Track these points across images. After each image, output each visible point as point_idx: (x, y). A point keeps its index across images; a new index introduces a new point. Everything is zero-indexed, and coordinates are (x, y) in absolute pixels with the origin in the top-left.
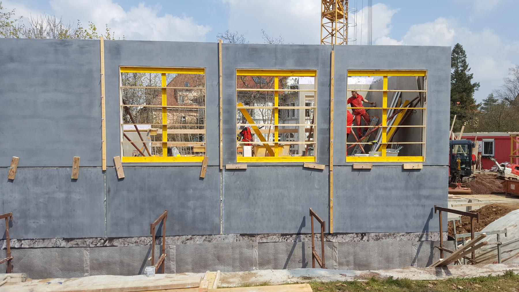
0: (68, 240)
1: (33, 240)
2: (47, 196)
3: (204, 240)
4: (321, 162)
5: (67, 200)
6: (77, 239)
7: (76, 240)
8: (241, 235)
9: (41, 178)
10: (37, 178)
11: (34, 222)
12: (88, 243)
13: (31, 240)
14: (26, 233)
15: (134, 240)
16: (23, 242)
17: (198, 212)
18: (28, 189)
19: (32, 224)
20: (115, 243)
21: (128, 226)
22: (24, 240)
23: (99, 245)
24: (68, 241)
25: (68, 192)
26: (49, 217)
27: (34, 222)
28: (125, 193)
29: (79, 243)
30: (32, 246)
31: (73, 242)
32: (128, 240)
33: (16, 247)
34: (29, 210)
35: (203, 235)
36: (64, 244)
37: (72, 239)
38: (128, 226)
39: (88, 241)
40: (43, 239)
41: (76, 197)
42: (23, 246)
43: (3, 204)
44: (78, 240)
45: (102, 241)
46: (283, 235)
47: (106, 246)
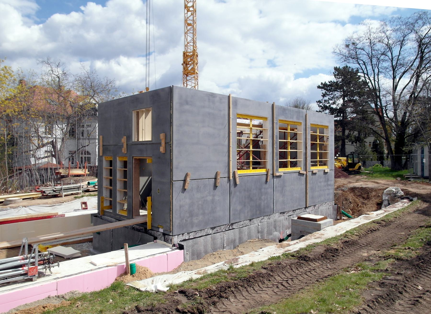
0: (213, 228)
1: (196, 231)
2: (203, 199)
3: (268, 219)
4: (303, 171)
5: (213, 201)
6: (217, 227)
7: (217, 228)
8: (281, 213)
9: (201, 187)
10: (199, 187)
11: (196, 219)
12: (222, 229)
13: (195, 232)
14: (192, 227)
15: (242, 223)
16: (190, 234)
17: (266, 202)
18: (193, 195)
19: (195, 221)
20: (234, 226)
21: (239, 214)
22: (191, 232)
23: (227, 229)
24: (213, 229)
25: (214, 196)
26: (204, 214)
27: (196, 219)
28: (238, 193)
29: (218, 230)
30: (195, 236)
31: (215, 230)
32: (239, 223)
33: (187, 239)
34: (194, 211)
35: (267, 216)
36: (211, 231)
37: (215, 228)
38: (239, 214)
39: (222, 227)
40: (201, 230)
41: (217, 198)
42: (190, 238)
43: (180, 208)
44: (217, 228)
45: (229, 226)
46: (293, 211)
47: (230, 230)
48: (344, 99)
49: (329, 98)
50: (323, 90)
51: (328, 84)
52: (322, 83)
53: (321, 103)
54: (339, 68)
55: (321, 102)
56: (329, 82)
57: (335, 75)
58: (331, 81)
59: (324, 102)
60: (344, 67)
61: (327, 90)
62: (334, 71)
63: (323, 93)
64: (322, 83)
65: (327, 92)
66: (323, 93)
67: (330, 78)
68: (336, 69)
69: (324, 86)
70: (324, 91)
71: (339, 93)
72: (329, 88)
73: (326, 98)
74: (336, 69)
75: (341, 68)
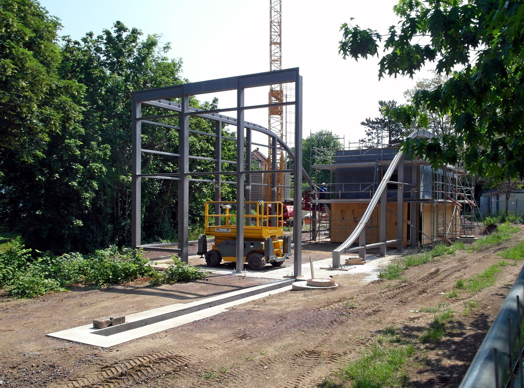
48: (390, 139)
49: (372, 137)
50: (366, 127)
51: (375, 121)
52: (367, 120)
53: (365, 142)
54: (385, 102)
55: (365, 142)
56: (376, 119)
57: (380, 110)
58: (378, 118)
59: (367, 141)
60: (390, 102)
61: (371, 127)
62: (380, 106)
63: (366, 131)
64: (367, 120)
65: (371, 129)
66: (366, 131)
67: (376, 114)
68: (381, 103)
69: (368, 123)
70: (367, 128)
71: (385, 132)
72: (374, 125)
73: (370, 137)
74: (381, 103)
75: (386, 102)
